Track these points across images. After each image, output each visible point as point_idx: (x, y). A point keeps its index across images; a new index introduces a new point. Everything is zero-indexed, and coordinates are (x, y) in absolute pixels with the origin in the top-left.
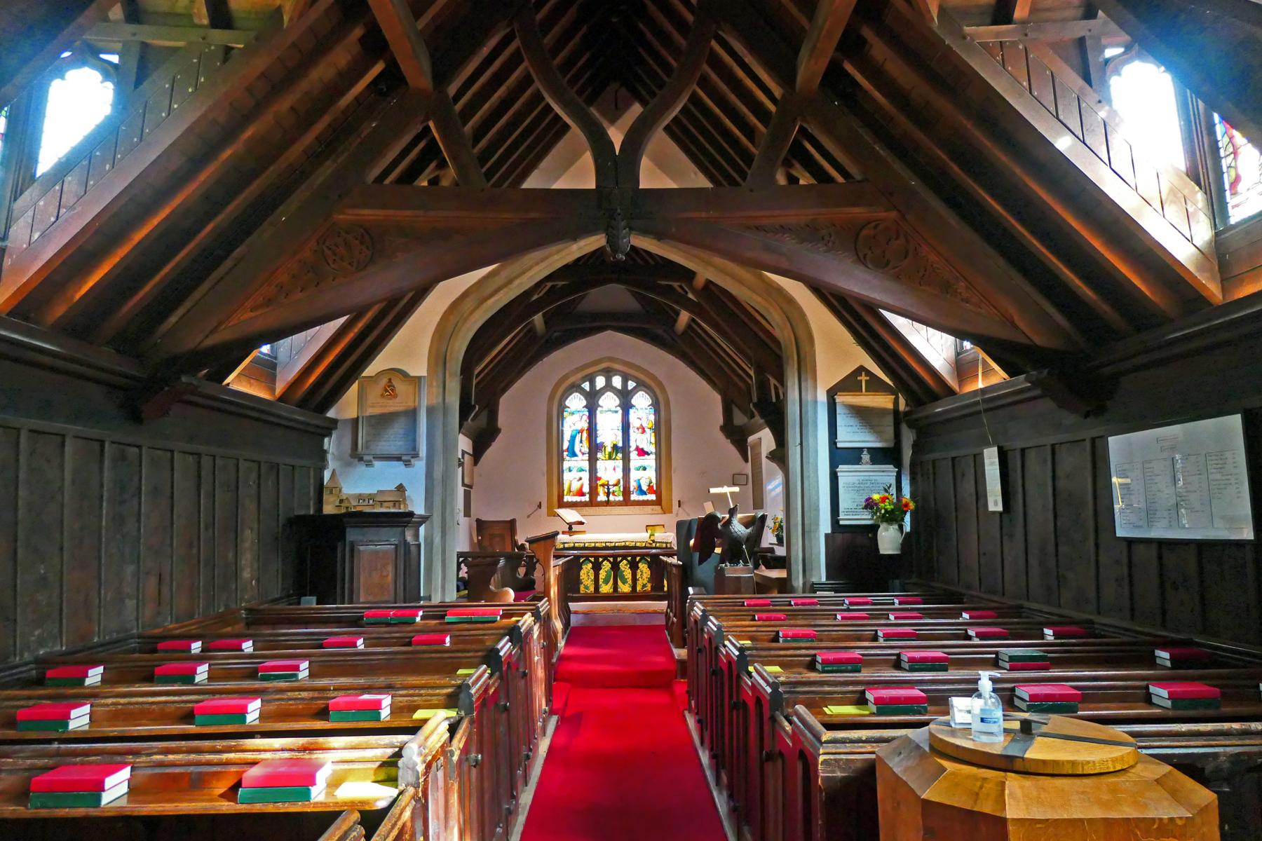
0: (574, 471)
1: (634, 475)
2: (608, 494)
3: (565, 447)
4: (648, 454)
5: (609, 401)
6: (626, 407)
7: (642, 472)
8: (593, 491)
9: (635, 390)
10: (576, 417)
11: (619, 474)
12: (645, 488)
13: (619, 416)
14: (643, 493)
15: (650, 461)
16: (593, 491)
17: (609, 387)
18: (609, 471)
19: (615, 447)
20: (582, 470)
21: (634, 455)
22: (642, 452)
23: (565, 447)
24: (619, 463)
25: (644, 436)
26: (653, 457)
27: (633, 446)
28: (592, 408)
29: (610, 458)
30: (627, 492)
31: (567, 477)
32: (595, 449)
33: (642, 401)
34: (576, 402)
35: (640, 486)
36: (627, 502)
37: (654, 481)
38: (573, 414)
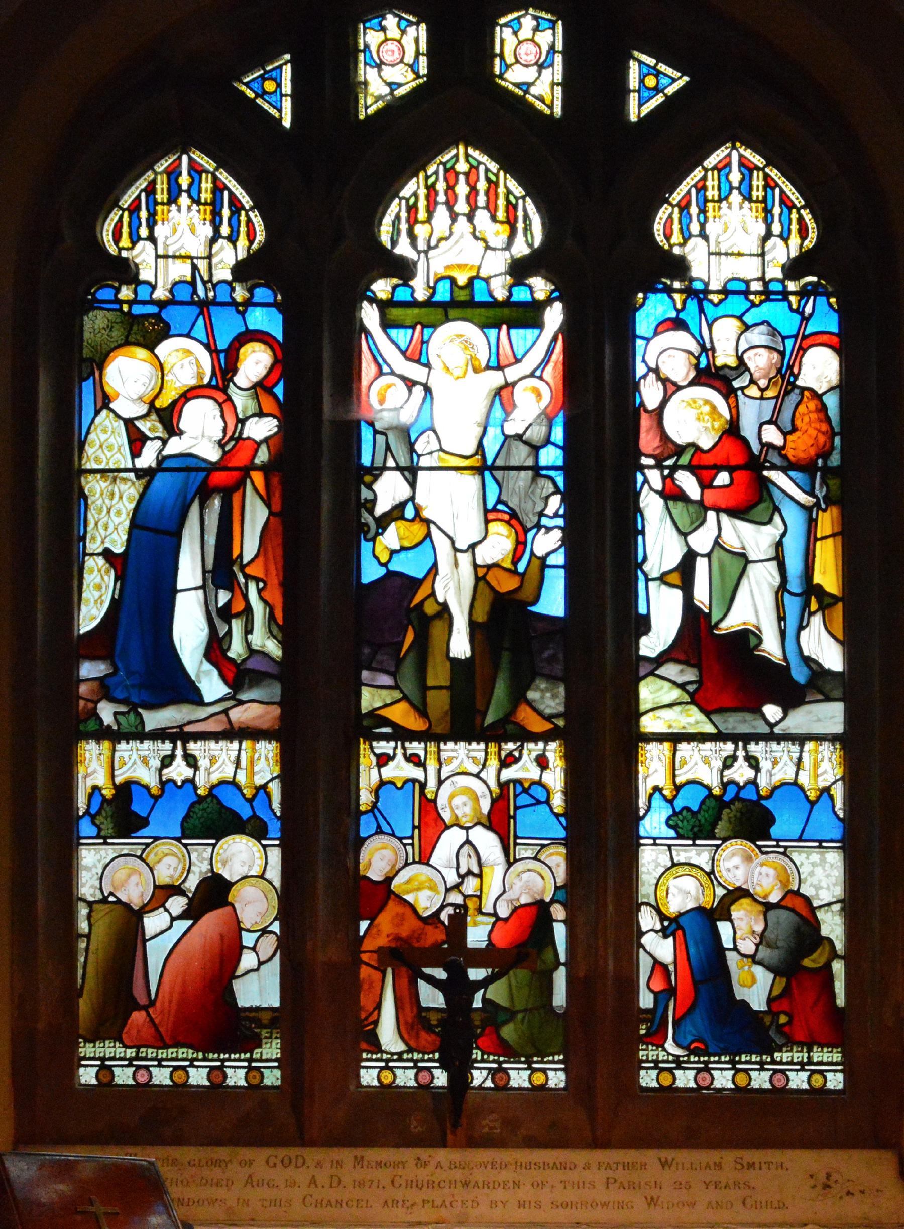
0: (166, 819)
1: (670, 876)
2: (451, 1035)
3: (91, 614)
4: (792, 697)
5: (462, 228)
6: (601, 270)
7: (736, 862)
8: (322, 1012)
9: (678, 140)
10: (185, 359)
11: (539, 875)
12: (755, 988)
13: (538, 348)
14: (734, 1029)
15: (804, 758)
16: (322, 1012)
17: (462, 100)
18: (463, 832)
19: (504, 611)
20: (212, 817)
21: (662, 704)
22: (734, 676)
23: (91, 614)
24: (544, 767)
25: (755, 538)
26: (830, 716)
27: (664, 614)
28: (320, 276)
29: (464, 725)
30: (602, 1027)
31: (99, 868)
32: (339, 634)
33: (734, 229)
34: (182, 234)
35: (709, 968)
36: (606, 1111)
37: (832, 926)
38: (148, 331)
